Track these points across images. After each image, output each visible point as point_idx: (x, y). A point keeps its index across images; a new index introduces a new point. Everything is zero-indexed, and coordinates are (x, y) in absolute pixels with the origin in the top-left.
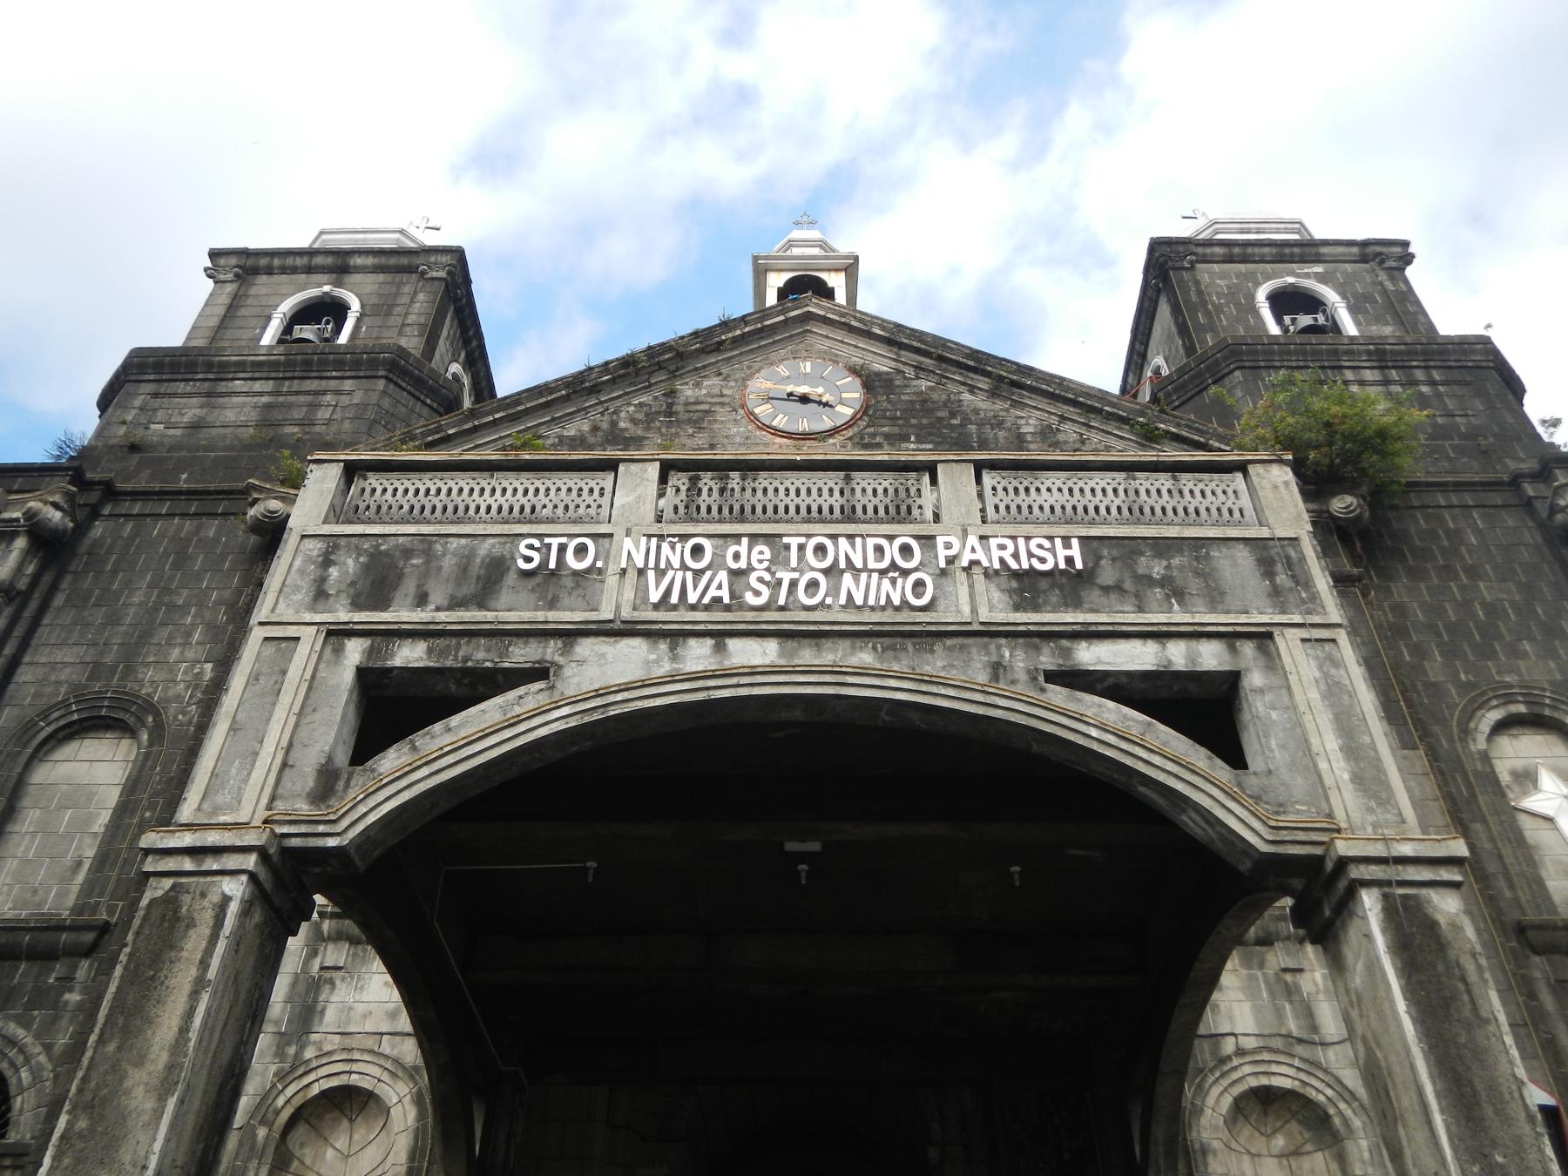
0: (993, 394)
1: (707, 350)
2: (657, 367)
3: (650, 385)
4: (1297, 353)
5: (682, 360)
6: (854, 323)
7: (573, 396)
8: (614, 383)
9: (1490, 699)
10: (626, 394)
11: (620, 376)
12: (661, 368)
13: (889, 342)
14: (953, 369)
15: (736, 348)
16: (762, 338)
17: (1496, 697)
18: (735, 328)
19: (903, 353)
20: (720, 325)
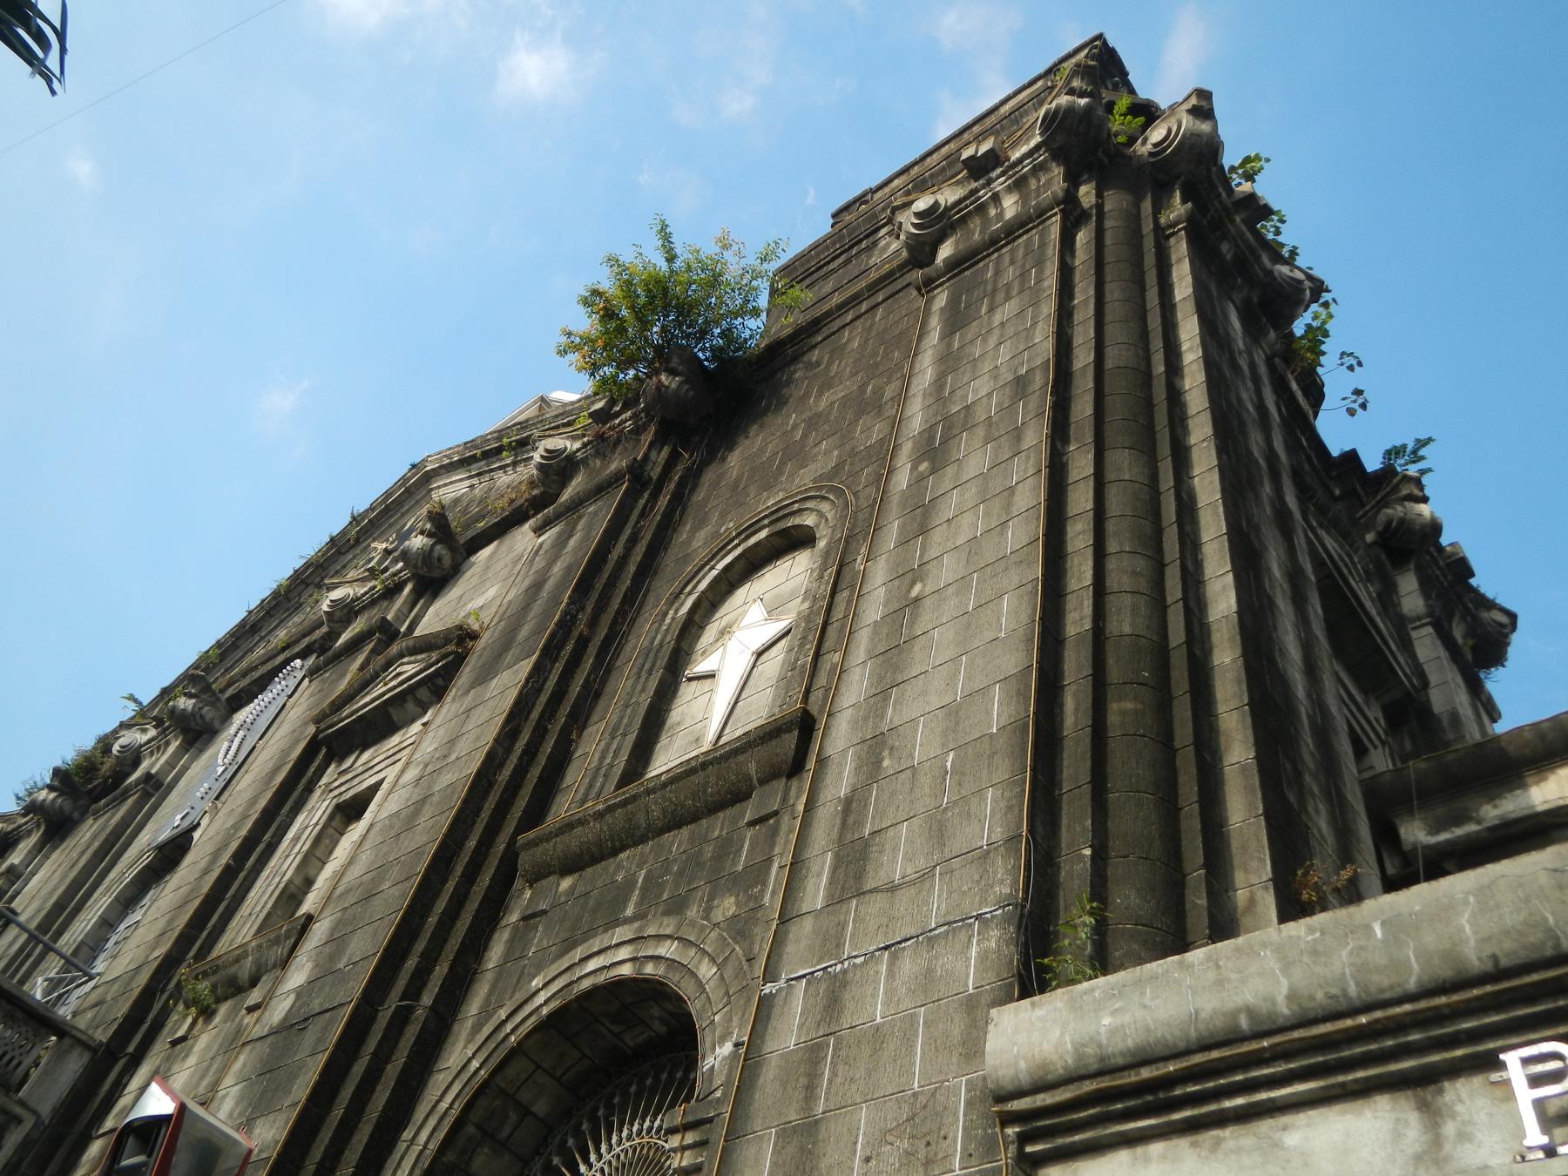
0: (515, 464)
1: (343, 550)
2: (303, 586)
3: (301, 605)
4: (834, 243)
5: (324, 570)
6: (447, 461)
7: (239, 643)
8: (272, 616)
9: (732, 540)
10: (280, 622)
11: (272, 608)
12: (308, 585)
13: (464, 463)
14: (494, 459)
15: (369, 537)
16: (391, 516)
17: (738, 535)
18: (363, 519)
19: (473, 467)
20: (351, 523)
